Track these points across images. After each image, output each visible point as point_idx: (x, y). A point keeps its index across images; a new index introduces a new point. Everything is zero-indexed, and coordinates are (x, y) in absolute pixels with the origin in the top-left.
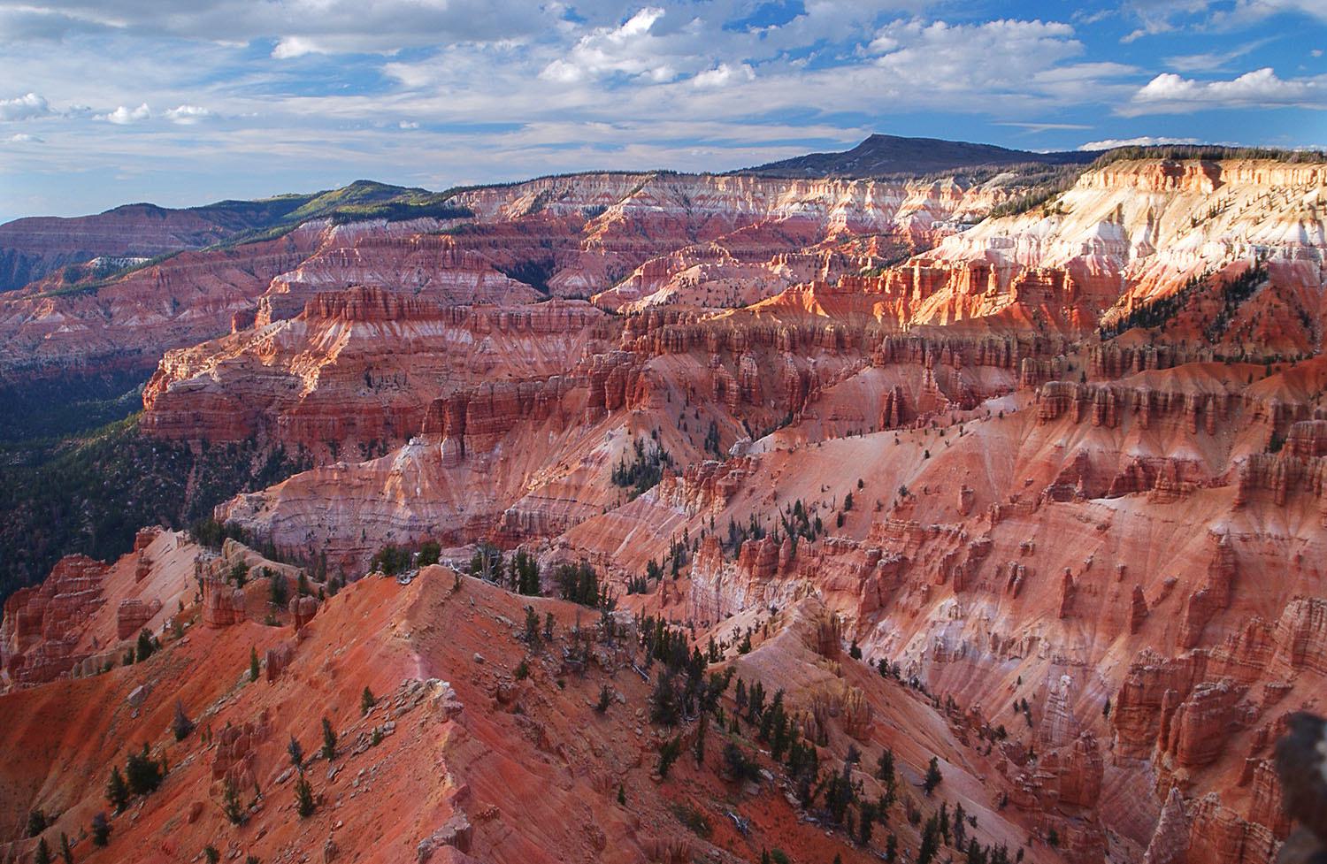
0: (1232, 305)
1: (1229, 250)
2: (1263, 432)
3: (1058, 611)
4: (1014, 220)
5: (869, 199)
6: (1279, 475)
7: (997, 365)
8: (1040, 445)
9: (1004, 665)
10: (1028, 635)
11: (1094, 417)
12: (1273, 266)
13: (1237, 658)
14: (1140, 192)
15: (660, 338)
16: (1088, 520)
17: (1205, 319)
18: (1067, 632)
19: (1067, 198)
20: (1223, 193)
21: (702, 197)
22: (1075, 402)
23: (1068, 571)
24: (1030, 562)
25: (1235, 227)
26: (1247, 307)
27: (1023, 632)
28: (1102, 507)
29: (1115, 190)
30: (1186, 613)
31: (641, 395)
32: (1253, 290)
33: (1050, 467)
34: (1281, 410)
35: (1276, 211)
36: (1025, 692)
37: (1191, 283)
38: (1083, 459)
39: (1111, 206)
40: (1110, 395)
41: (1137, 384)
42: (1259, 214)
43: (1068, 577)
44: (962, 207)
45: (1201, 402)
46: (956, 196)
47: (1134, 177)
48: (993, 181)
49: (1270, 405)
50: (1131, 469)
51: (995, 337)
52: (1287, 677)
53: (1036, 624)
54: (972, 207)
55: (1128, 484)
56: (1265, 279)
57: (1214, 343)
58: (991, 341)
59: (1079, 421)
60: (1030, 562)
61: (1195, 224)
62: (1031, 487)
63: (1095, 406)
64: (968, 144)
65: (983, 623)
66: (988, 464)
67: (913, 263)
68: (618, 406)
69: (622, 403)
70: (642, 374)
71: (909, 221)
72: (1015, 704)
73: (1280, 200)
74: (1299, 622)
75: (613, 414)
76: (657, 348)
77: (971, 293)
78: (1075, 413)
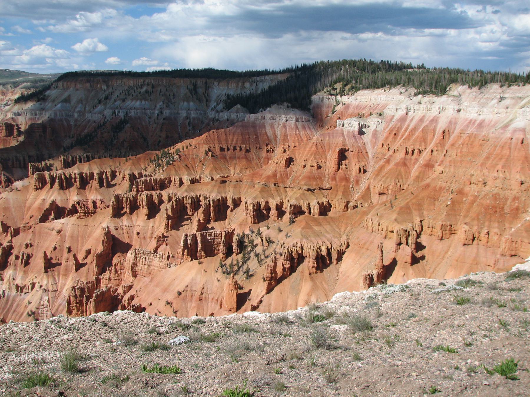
0: (116, 134)
1: (114, 113)
2: (126, 184)
3: (43, 270)
6: (127, 202)
7: (20, 167)
8: (35, 199)
9: (22, 297)
10: (31, 282)
11: (56, 185)
12: (130, 117)
13: (112, 277)
14: (77, 90)
16: (53, 229)
17: (106, 141)
18: (48, 278)
19: (47, 93)
20: (110, 90)
22: (48, 180)
23: (45, 252)
24: (29, 251)
25: (116, 103)
26: (122, 135)
27: (28, 282)
28: (58, 223)
29: (68, 88)
30: (95, 262)
32: (123, 128)
33: (39, 208)
34: (132, 176)
35: (131, 97)
36: (32, 307)
37: (99, 126)
38: (53, 203)
39: (66, 95)
40: (63, 176)
41: (75, 171)
42: (124, 97)
43: (45, 255)
44: (7, 98)
45: (101, 174)
47: (73, 84)
48: (21, 86)
49: (127, 173)
50: (74, 206)
51: (18, 155)
52: (131, 281)
53: (34, 277)
55: (73, 211)
56: (128, 123)
57: (110, 150)
58: (16, 157)
59: (51, 187)
60: (29, 251)
61: (100, 102)
62: (32, 219)
63: (57, 181)
65: (11, 280)
66: (13, 210)
72: (28, 313)
73: (132, 91)
74: (132, 259)
77: (7, 136)
78: (49, 185)
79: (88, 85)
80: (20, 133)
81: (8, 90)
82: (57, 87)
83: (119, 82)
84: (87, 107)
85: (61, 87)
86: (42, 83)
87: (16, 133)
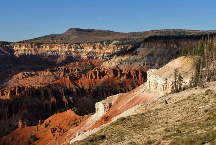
4: (123, 57)
5: (73, 50)
14: (158, 48)
15: (27, 93)
20: (180, 48)
21: (17, 50)
29: (151, 47)
31: (24, 109)
44: (103, 52)
46: (101, 48)
47: (155, 44)
48: (112, 43)
54: (106, 51)
58: (121, 90)
64: (102, 30)
67: (95, 69)
68: (16, 112)
69: (18, 112)
70: (24, 103)
71: (87, 56)
75: (15, 115)
76: (26, 96)
79: (165, 45)
80: (122, 75)
81: (104, 46)
82: (144, 46)
83: (185, 43)
84: (164, 59)
85: (147, 46)
86: (127, 41)
87: (119, 75)
